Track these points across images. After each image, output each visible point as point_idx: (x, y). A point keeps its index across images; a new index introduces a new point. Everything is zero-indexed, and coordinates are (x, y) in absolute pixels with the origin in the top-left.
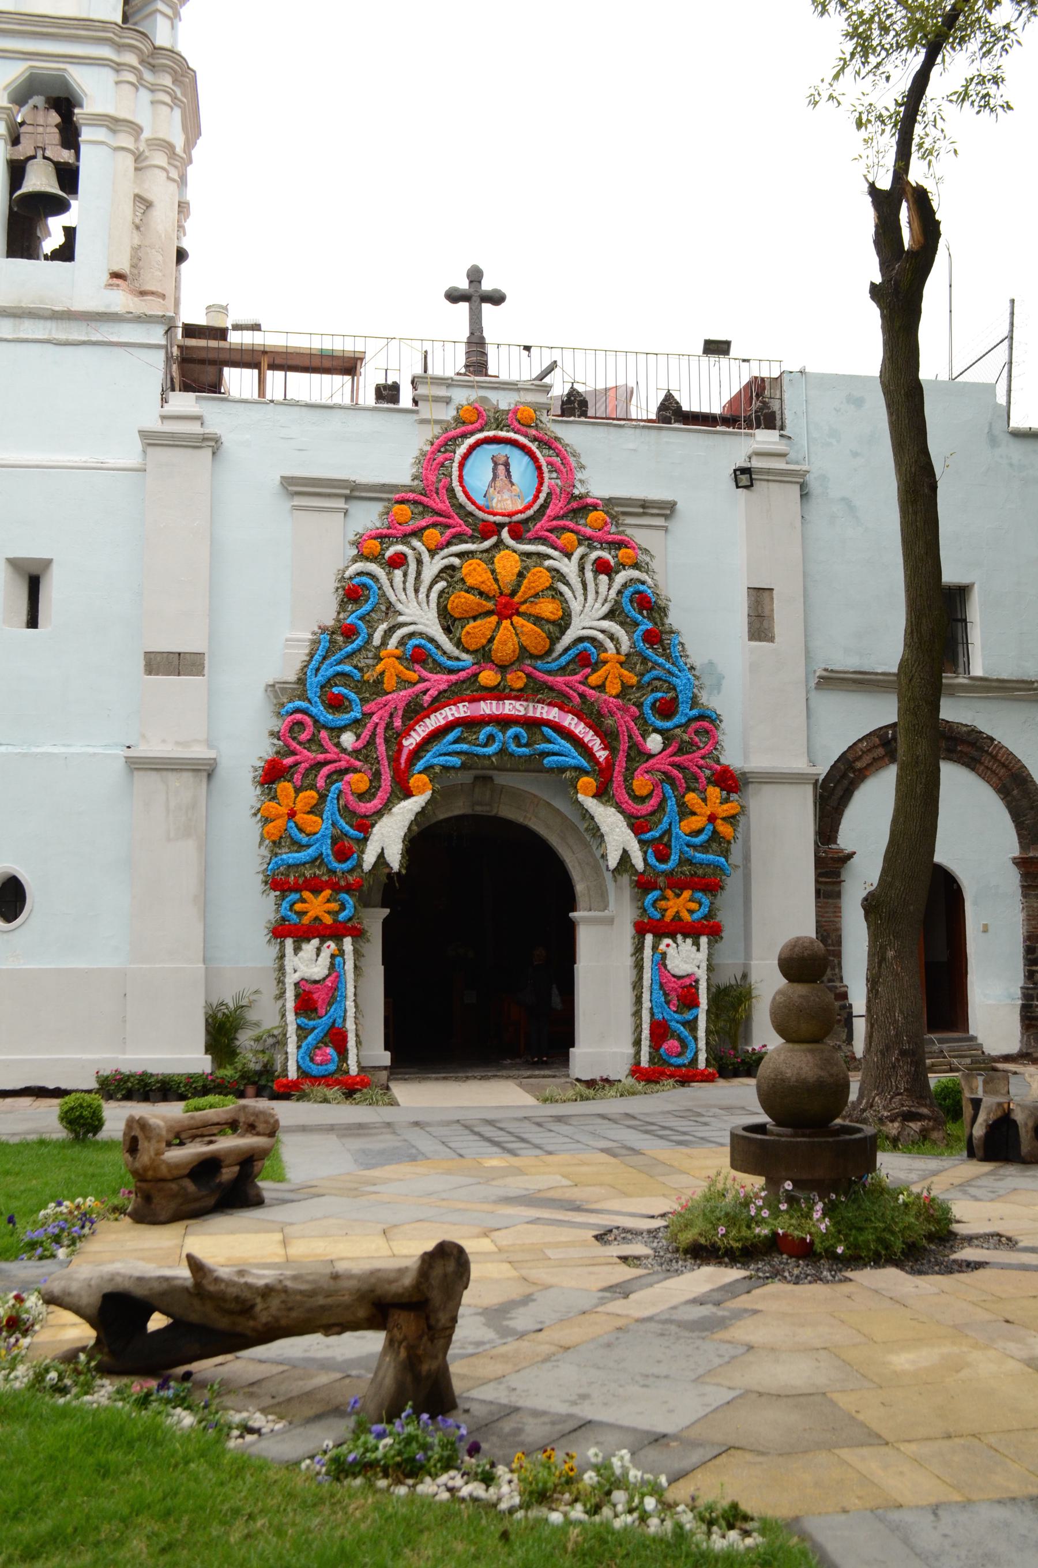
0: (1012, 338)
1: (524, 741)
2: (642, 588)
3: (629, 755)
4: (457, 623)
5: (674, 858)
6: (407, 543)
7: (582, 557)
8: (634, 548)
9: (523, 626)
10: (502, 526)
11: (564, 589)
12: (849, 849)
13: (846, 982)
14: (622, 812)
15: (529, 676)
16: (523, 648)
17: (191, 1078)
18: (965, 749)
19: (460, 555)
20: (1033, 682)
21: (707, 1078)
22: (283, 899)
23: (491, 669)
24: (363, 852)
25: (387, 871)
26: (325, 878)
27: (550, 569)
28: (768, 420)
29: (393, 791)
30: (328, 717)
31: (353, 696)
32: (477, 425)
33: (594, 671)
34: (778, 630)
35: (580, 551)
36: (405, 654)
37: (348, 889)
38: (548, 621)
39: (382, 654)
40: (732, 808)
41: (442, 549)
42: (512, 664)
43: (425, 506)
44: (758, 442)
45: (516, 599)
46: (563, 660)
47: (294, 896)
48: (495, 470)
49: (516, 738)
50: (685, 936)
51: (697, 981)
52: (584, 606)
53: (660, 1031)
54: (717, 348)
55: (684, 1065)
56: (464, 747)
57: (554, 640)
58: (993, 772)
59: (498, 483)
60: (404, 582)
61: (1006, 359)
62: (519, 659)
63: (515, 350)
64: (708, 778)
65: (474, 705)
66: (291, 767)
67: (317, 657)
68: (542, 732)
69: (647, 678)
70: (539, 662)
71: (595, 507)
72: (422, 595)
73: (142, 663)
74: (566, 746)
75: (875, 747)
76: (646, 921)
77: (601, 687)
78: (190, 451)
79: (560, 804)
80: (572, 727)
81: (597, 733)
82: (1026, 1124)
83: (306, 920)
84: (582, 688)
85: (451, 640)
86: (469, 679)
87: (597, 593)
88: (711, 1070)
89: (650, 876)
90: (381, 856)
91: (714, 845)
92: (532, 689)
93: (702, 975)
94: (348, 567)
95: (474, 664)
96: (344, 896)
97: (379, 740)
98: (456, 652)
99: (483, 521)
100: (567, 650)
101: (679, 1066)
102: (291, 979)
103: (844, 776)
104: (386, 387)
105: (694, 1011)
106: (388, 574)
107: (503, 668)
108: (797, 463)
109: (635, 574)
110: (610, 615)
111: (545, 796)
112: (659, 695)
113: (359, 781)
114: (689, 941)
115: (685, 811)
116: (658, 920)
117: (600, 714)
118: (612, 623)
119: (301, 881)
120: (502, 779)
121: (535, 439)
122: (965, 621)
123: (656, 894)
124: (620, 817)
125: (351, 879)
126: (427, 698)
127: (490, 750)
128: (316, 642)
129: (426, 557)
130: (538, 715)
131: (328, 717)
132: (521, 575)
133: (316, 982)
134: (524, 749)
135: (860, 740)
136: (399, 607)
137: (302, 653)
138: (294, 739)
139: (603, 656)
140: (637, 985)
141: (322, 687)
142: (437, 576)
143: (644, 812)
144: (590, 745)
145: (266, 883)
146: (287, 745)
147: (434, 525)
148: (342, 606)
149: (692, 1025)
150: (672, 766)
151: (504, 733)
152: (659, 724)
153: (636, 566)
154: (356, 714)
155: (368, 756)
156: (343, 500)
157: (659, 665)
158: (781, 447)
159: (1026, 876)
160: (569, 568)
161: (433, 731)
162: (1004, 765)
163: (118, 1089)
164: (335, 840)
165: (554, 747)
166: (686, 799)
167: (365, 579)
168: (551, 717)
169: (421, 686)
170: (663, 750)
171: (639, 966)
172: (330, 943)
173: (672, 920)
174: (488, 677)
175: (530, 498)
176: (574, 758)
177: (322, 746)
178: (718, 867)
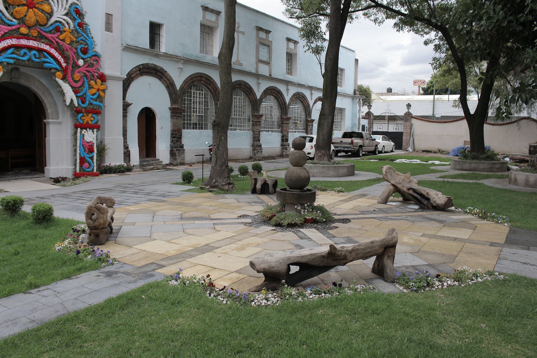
1: (37, 56)
2: (77, 6)
3: (72, 66)
5: (87, 102)
9: (37, 13)
12: (130, 102)
13: (128, 143)
14: (71, 86)
15: (38, 32)
16: (37, 21)
20: (178, 56)
21: (96, 175)
23: (25, 27)
33: (61, 34)
34: (113, 29)
38: (47, 12)
40: (104, 87)
42: (33, 26)
46: (51, 28)
49: (35, 55)
50: (90, 129)
51: (93, 144)
52: (58, 9)
53: (83, 160)
55: (90, 171)
56: (15, 56)
57: (48, 20)
58: (166, 81)
62: (35, 25)
64: (97, 76)
65: (19, 40)
68: (43, 54)
69: (79, 39)
70: (42, 27)
74: (51, 60)
75: (137, 71)
76: (78, 123)
77: (63, 40)
79: (43, 81)
80: (54, 53)
81: (62, 57)
82: (271, 184)
84: (57, 40)
86: (16, 29)
87: (62, 5)
88: (98, 172)
89: (80, 108)
91: (98, 100)
92: (39, 37)
93: (95, 141)
95: (18, 24)
100: (51, 25)
101: (88, 172)
103: (128, 79)
105: (93, 154)
107: (29, 27)
110: (66, 15)
111: (37, 76)
112: (83, 46)
114: (91, 130)
115: (91, 87)
116: (82, 123)
118: (67, 18)
120: (22, 69)
122: (159, 35)
123: (81, 115)
124: (70, 87)
127: (25, 58)
130: (42, 47)
134: (37, 59)
135: (134, 68)
139: (64, 29)
140: (75, 145)
143: (78, 86)
144: (60, 61)
149: (92, 158)
150: (86, 71)
157: (83, 35)
159: (172, 113)
161: (3, 48)
162: (168, 80)
165: (47, 60)
166: (90, 83)
168: (46, 49)
170: (84, 65)
171: (76, 140)
173: (86, 123)
174: (24, 30)
176: (55, 65)
178: (100, 106)
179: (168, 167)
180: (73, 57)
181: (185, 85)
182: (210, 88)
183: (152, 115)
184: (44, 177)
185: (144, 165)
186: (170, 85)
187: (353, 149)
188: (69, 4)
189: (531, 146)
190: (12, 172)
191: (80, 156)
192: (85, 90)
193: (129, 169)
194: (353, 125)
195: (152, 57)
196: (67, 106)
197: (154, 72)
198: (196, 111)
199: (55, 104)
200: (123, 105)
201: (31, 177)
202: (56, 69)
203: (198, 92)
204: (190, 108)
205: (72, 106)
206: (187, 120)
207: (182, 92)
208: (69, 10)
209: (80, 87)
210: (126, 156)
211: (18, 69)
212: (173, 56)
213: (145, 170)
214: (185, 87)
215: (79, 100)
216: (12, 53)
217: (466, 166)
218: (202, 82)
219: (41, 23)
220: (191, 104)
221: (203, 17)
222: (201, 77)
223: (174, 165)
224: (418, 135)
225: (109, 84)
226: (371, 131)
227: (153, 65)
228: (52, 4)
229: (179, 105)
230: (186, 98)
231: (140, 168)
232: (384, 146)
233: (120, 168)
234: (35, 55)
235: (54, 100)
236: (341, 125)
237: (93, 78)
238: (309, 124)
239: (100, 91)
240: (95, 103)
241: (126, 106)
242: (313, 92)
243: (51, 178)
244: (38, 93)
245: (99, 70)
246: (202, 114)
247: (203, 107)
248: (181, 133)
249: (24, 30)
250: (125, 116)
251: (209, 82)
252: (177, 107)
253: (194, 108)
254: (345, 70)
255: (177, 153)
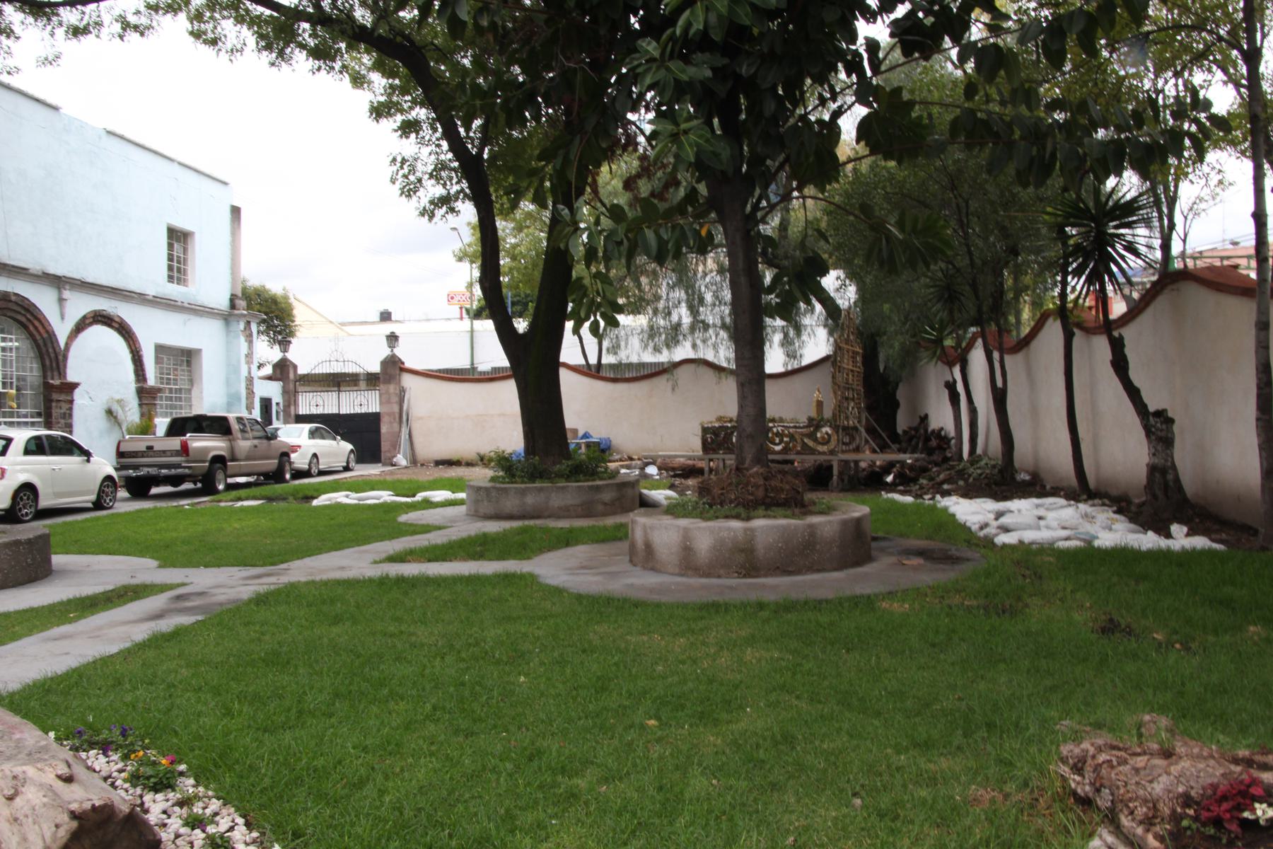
187: (187, 471)
189: (705, 430)
194: (232, 401)
217: (510, 504)
224: (421, 418)
226: (293, 413)
232: (315, 455)
236: (190, 400)
238: (55, 396)
242: (67, 294)
254: (197, 237)
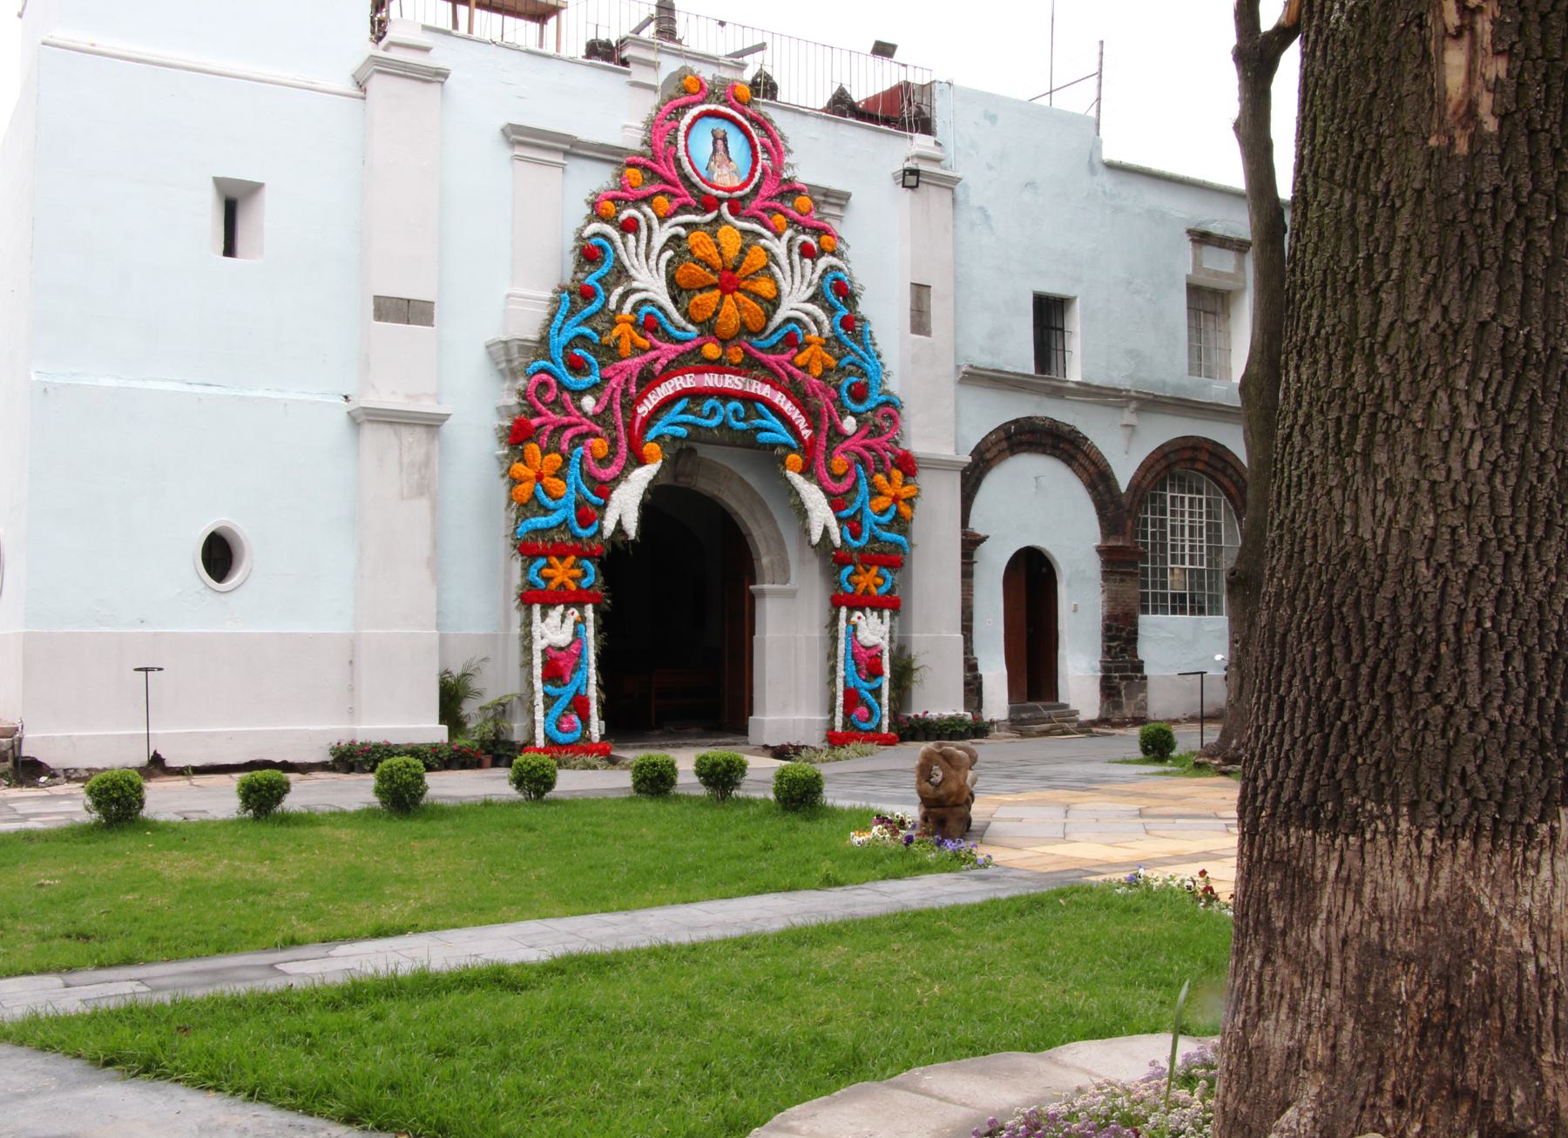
0: (1100, 77)
1: (742, 415)
2: (841, 275)
4: (684, 293)
5: (866, 535)
6: (638, 209)
7: (791, 240)
8: (832, 236)
9: (744, 302)
10: (720, 200)
11: (775, 269)
13: (976, 655)
15: (745, 351)
16: (743, 324)
17: (435, 748)
18: (1067, 447)
19: (686, 225)
20: (1121, 391)
21: (887, 741)
22: (531, 564)
24: (603, 518)
25: (623, 538)
26: (570, 543)
27: (766, 249)
28: (925, 125)
29: (627, 459)
30: (569, 379)
31: (592, 359)
32: (699, 97)
33: (800, 352)
34: (934, 325)
35: (788, 233)
36: (637, 320)
37: (589, 557)
39: (618, 318)
41: (670, 217)
42: (733, 338)
43: (654, 172)
44: (919, 146)
45: (737, 275)
46: (775, 339)
47: (541, 562)
48: (715, 143)
49: (736, 412)
50: (873, 609)
51: (881, 652)
53: (852, 698)
54: (883, 50)
55: (872, 730)
56: (690, 418)
57: (769, 318)
58: (1085, 468)
59: (718, 158)
60: (637, 247)
61: (1095, 97)
63: (715, 23)
65: (699, 376)
66: (537, 428)
67: (560, 317)
68: (755, 408)
69: (844, 362)
71: (799, 192)
72: (652, 263)
73: (370, 308)
74: (774, 422)
77: (805, 368)
78: (419, 85)
79: (752, 479)
80: (782, 405)
81: (802, 413)
83: (553, 585)
84: (791, 368)
85: (678, 310)
86: (693, 350)
87: (803, 276)
88: (893, 734)
90: (619, 523)
91: (896, 527)
93: (885, 645)
94: (585, 226)
96: (587, 563)
97: (617, 407)
98: (683, 323)
99: (705, 193)
100: (776, 330)
101: (866, 731)
102: (538, 646)
104: (601, 44)
105: (879, 680)
106: (623, 236)
107: (724, 342)
108: (945, 169)
109: (834, 261)
110: (812, 299)
112: (854, 379)
113: (600, 446)
114: (875, 614)
115: (875, 492)
117: (806, 395)
119: (549, 546)
120: (705, 452)
121: (752, 120)
122: (1062, 330)
124: (821, 494)
125: (594, 546)
126: (658, 367)
128: (556, 302)
129: (655, 223)
130: (753, 391)
131: (569, 379)
132: (742, 251)
133: (561, 649)
135: (991, 433)
136: (632, 272)
137: (543, 313)
138: (539, 399)
139: (807, 337)
140: (832, 655)
141: (565, 348)
142: (665, 245)
143: (841, 490)
145: (515, 547)
146: (532, 405)
147: (663, 193)
148: (579, 266)
149: (877, 693)
151: (724, 406)
152: (853, 407)
153: (833, 254)
154: (595, 378)
155: (605, 421)
156: (562, 155)
157: (853, 350)
158: (936, 153)
159: (1105, 563)
160: (779, 248)
162: (1094, 463)
163: (367, 759)
164: (578, 505)
167: (601, 241)
168: (763, 394)
169: (653, 354)
172: (573, 610)
174: (712, 350)
175: (745, 177)
177: (563, 408)
178: (899, 545)
179: (1094, 730)
180: (830, 411)
181: (1144, 477)
182: (1225, 481)
183: (1044, 570)
184: (748, 744)
185: (1022, 719)
186: (1097, 477)
188: (819, 271)
190: (658, 732)
191: (845, 686)
192: (859, 499)
193: (979, 730)
195: (1045, 399)
196: (813, 547)
197: (1049, 441)
198: (1183, 556)
199: (781, 543)
200: (963, 541)
201: (714, 741)
202: (786, 446)
203: (1187, 496)
204: (1163, 548)
205: (826, 546)
206: (1154, 586)
207: (1136, 499)
208: (820, 287)
209: (848, 492)
210: (971, 690)
211: (692, 451)
212: (1104, 392)
213: (1023, 735)
214: (1145, 483)
215: (846, 528)
216: (683, 412)
218: (1200, 466)
219: (753, 329)
220: (1164, 535)
221: (1194, 264)
222: (1194, 448)
223: (1114, 725)
225: (924, 479)
227: (1047, 422)
228: (779, 275)
229: (1128, 538)
230: (1149, 516)
231: (1011, 729)
233: (953, 726)
234: (736, 412)
235: (777, 530)
237: (881, 466)
239: (901, 503)
240: (887, 536)
241: (971, 544)
243: (766, 747)
244: (737, 514)
245: (897, 443)
246: (1201, 564)
247: (1205, 544)
248: (1135, 625)
249: (712, 350)
250: (967, 574)
251: (1220, 465)
252: (1120, 544)
253: (1174, 547)
255: (1122, 687)
